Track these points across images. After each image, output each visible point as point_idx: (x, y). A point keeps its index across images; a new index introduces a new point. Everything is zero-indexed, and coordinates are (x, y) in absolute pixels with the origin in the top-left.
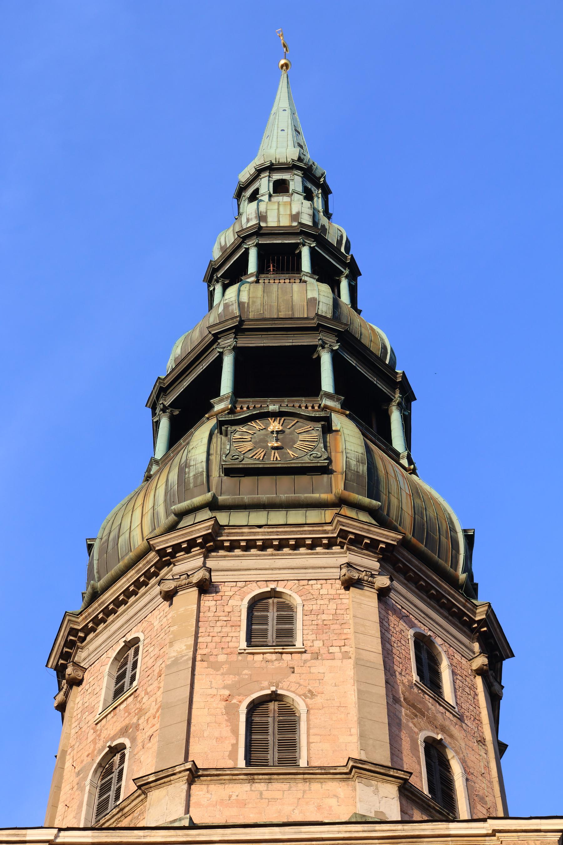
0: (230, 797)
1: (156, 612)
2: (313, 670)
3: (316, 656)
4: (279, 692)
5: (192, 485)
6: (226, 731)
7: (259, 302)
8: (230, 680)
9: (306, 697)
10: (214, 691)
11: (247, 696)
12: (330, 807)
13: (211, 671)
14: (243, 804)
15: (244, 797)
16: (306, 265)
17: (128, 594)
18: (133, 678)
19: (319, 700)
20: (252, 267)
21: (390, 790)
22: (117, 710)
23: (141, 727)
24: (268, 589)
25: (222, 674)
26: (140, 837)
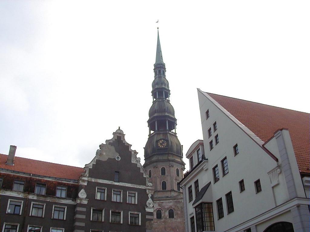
6: (160, 185)
19: (168, 182)
21: (173, 192)
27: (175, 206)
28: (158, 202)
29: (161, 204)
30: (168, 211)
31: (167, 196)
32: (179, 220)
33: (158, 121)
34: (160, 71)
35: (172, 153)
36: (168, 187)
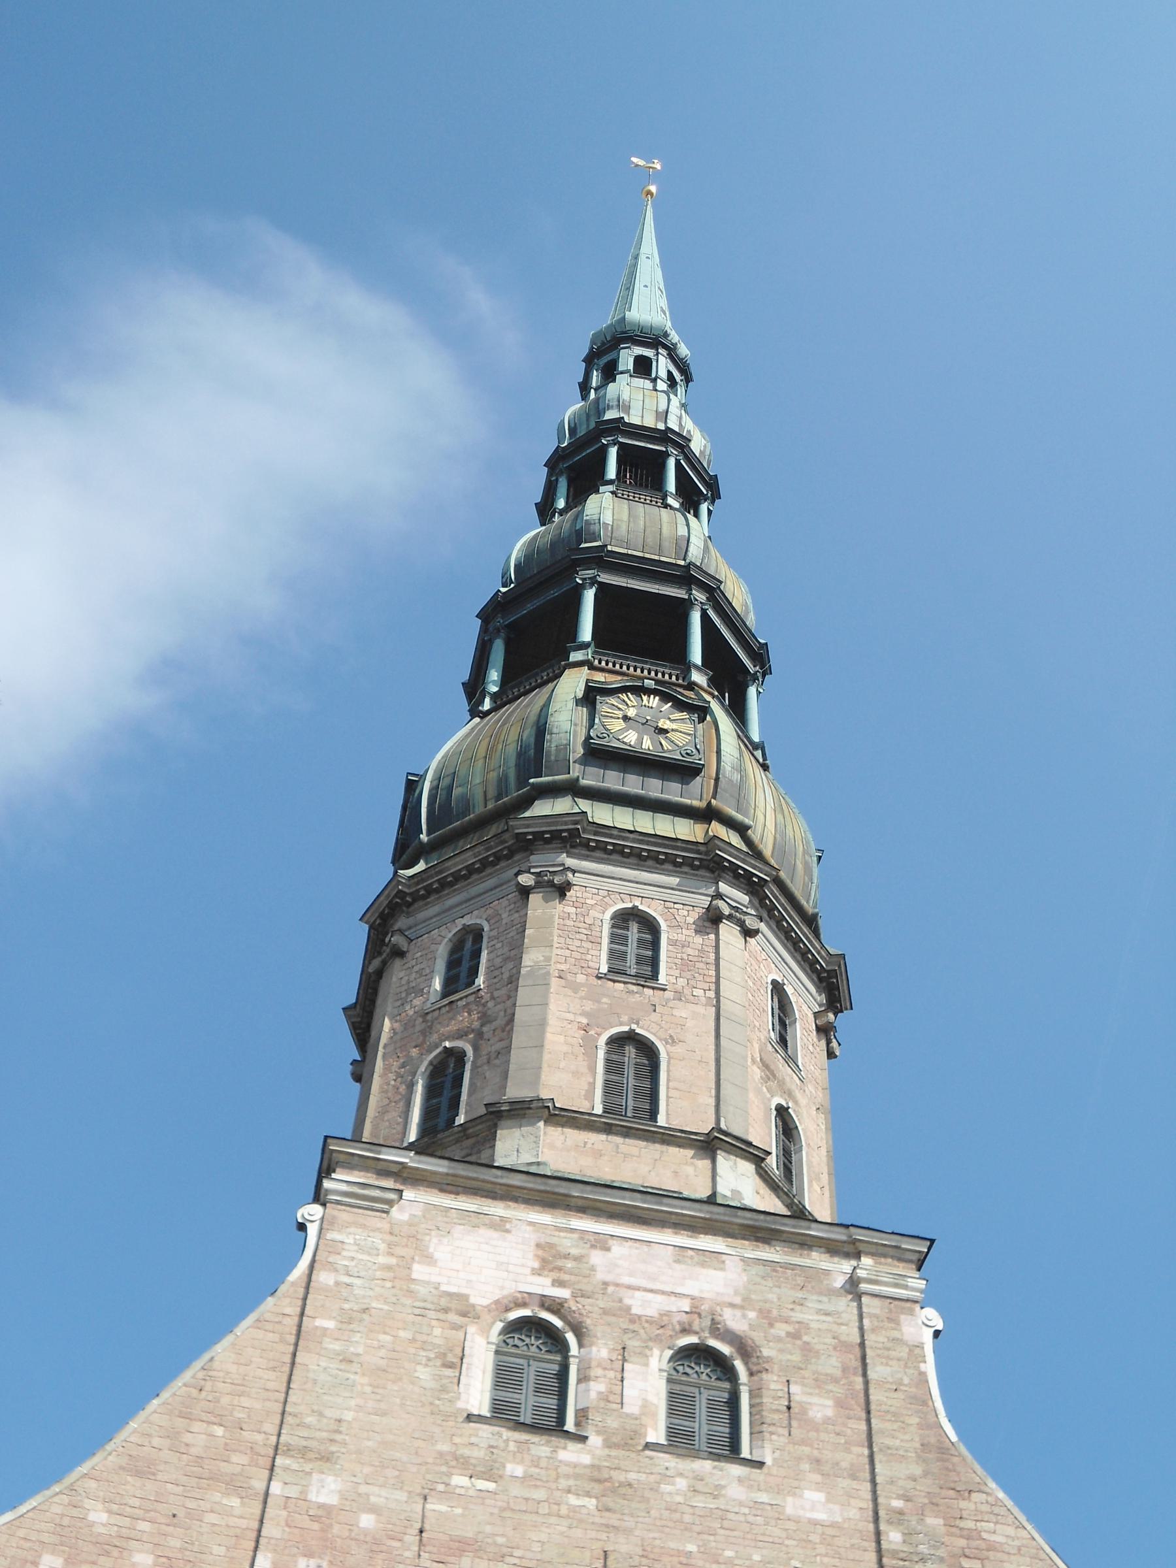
0: (586, 1143)
1: (504, 902)
2: (675, 1012)
3: (679, 995)
4: (638, 1031)
5: (553, 758)
6: (582, 1064)
7: (624, 527)
8: (589, 1006)
9: (667, 1043)
10: (570, 1016)
11: (606, 1029)
12: (687, 1176)
13: (569, 992)
14: (598, 1154)
15: (601, 1148)
16: (671, 485)
17: (471, 871)
18: (474, 972)
19: (678, 1049)
20: (611, 472)
21: (747, 1168)
22: (454, 1006)
23: (486, 1037)
24: (630, 905)
25: (582, 998)
26: (497, 1177)
27: (768, 1318)
28: (544, 1218)
29: (578, 1259)
30: (659, 1360)
31: (670, 1185)
32: (813, 1503)
33: (604, 592)
34: (643, 367)
35: (747, 821)
36: (682, 1103)
